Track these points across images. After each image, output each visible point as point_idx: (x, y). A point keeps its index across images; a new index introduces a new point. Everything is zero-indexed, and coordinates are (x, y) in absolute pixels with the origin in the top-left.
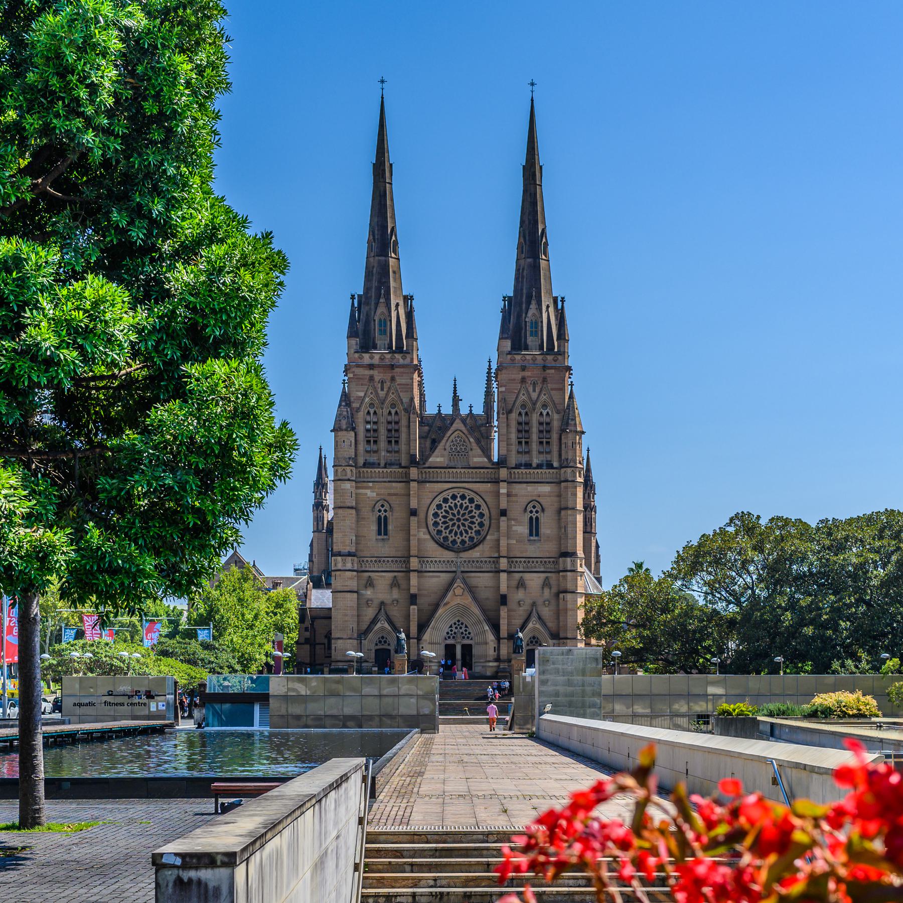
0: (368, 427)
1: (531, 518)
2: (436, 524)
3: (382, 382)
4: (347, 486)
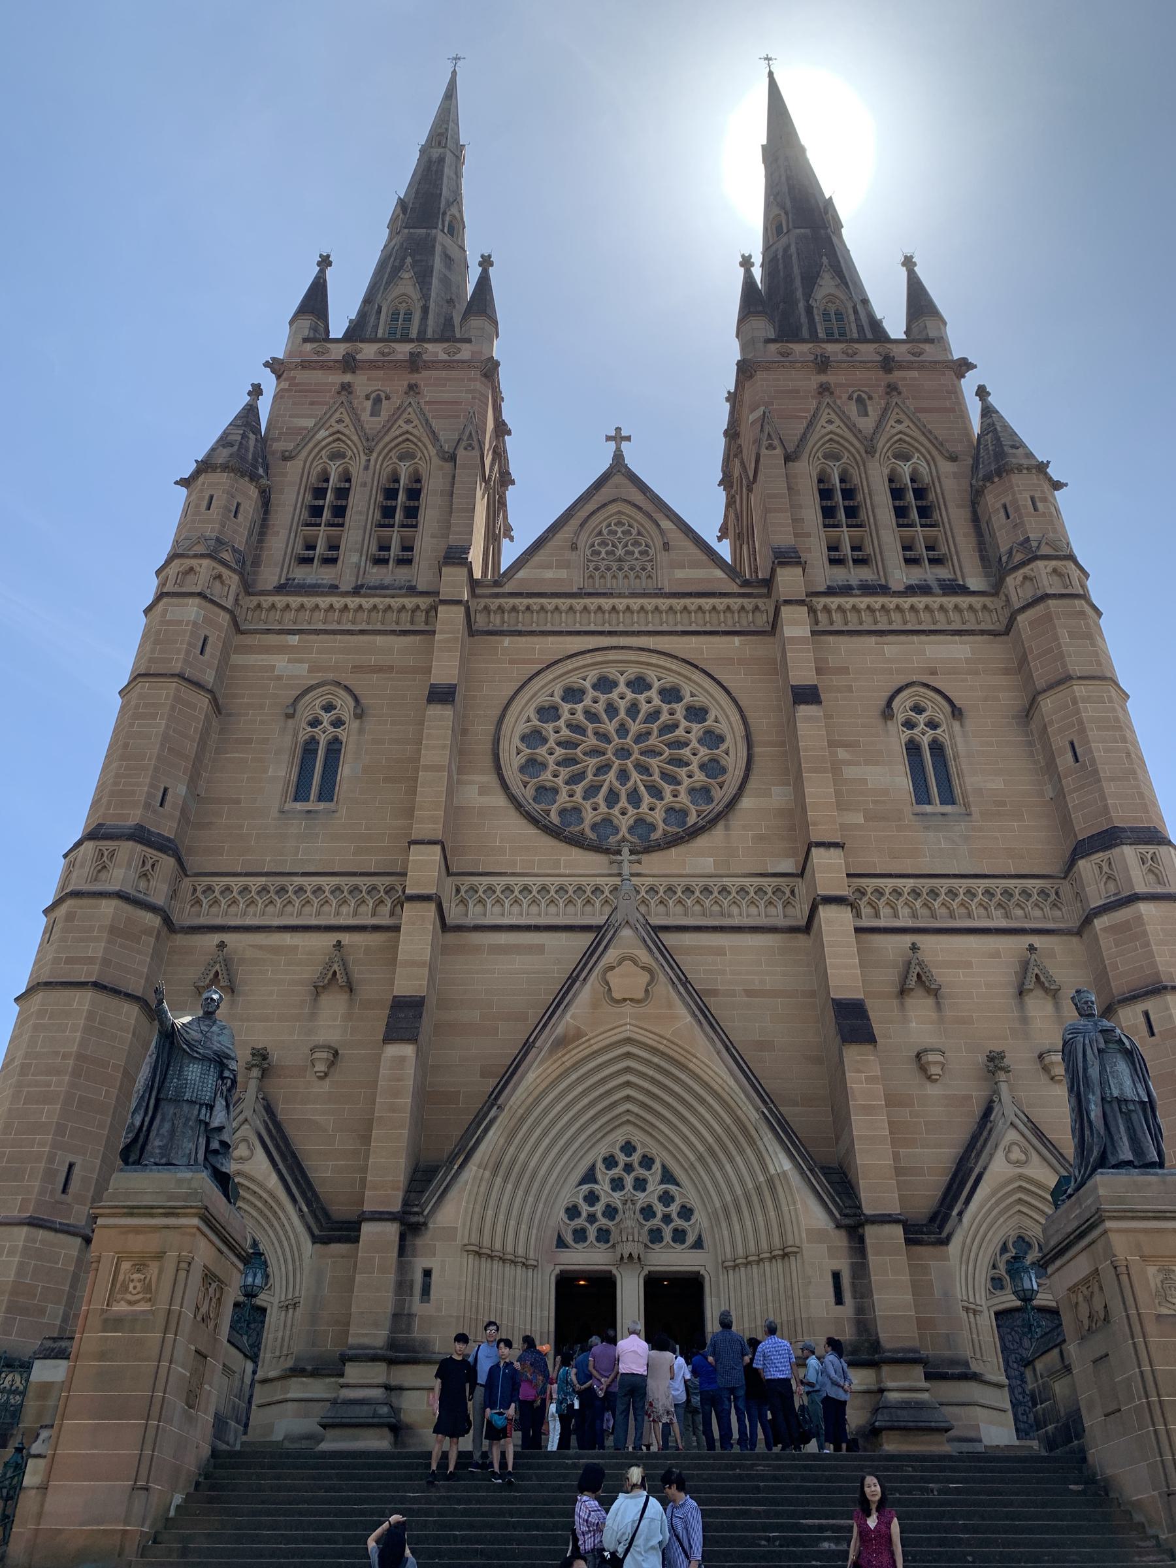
1: (913, 748)
2: (532, 765)
4: (191, 610)
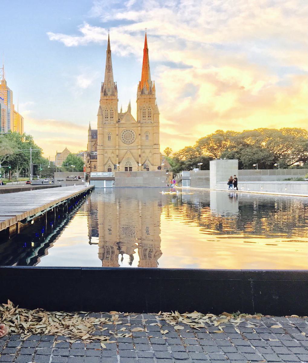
0: (106, 114)
1: (146, 136)
3: (109, 103)
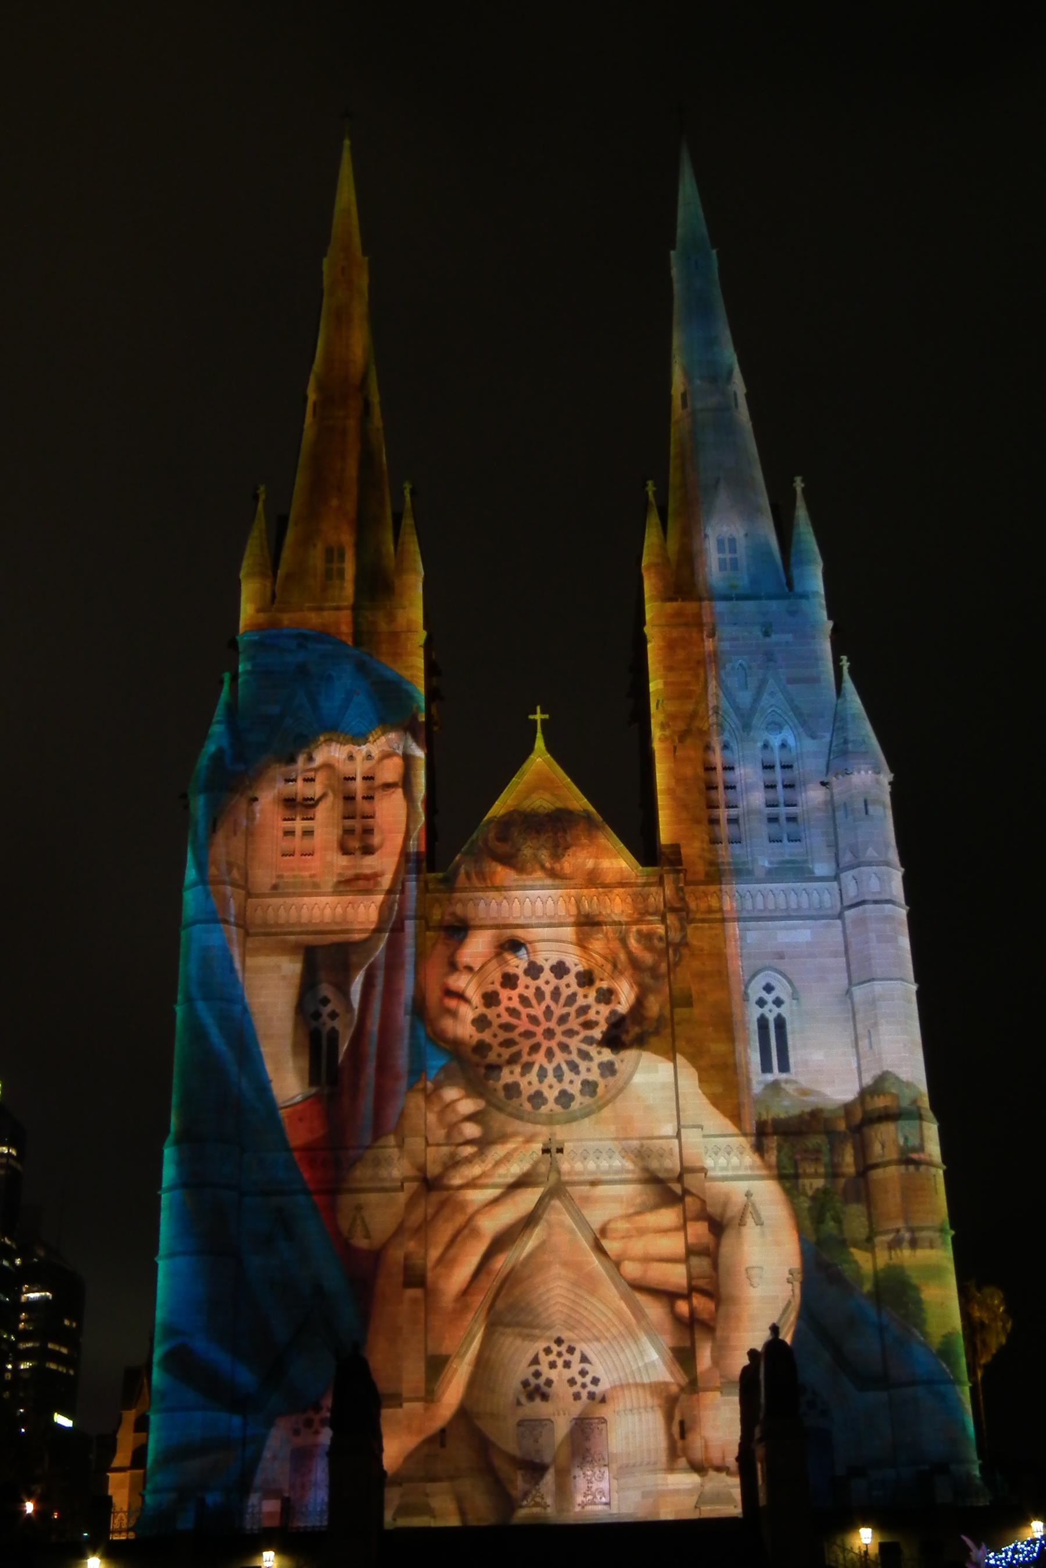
1: (763, 1023)
